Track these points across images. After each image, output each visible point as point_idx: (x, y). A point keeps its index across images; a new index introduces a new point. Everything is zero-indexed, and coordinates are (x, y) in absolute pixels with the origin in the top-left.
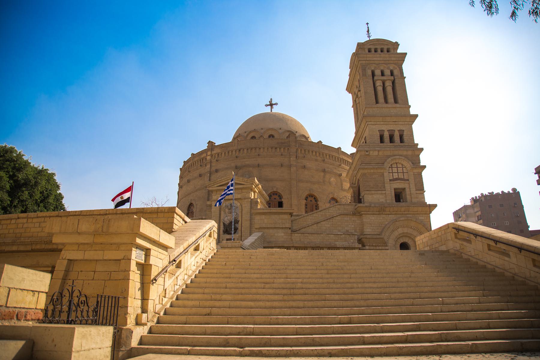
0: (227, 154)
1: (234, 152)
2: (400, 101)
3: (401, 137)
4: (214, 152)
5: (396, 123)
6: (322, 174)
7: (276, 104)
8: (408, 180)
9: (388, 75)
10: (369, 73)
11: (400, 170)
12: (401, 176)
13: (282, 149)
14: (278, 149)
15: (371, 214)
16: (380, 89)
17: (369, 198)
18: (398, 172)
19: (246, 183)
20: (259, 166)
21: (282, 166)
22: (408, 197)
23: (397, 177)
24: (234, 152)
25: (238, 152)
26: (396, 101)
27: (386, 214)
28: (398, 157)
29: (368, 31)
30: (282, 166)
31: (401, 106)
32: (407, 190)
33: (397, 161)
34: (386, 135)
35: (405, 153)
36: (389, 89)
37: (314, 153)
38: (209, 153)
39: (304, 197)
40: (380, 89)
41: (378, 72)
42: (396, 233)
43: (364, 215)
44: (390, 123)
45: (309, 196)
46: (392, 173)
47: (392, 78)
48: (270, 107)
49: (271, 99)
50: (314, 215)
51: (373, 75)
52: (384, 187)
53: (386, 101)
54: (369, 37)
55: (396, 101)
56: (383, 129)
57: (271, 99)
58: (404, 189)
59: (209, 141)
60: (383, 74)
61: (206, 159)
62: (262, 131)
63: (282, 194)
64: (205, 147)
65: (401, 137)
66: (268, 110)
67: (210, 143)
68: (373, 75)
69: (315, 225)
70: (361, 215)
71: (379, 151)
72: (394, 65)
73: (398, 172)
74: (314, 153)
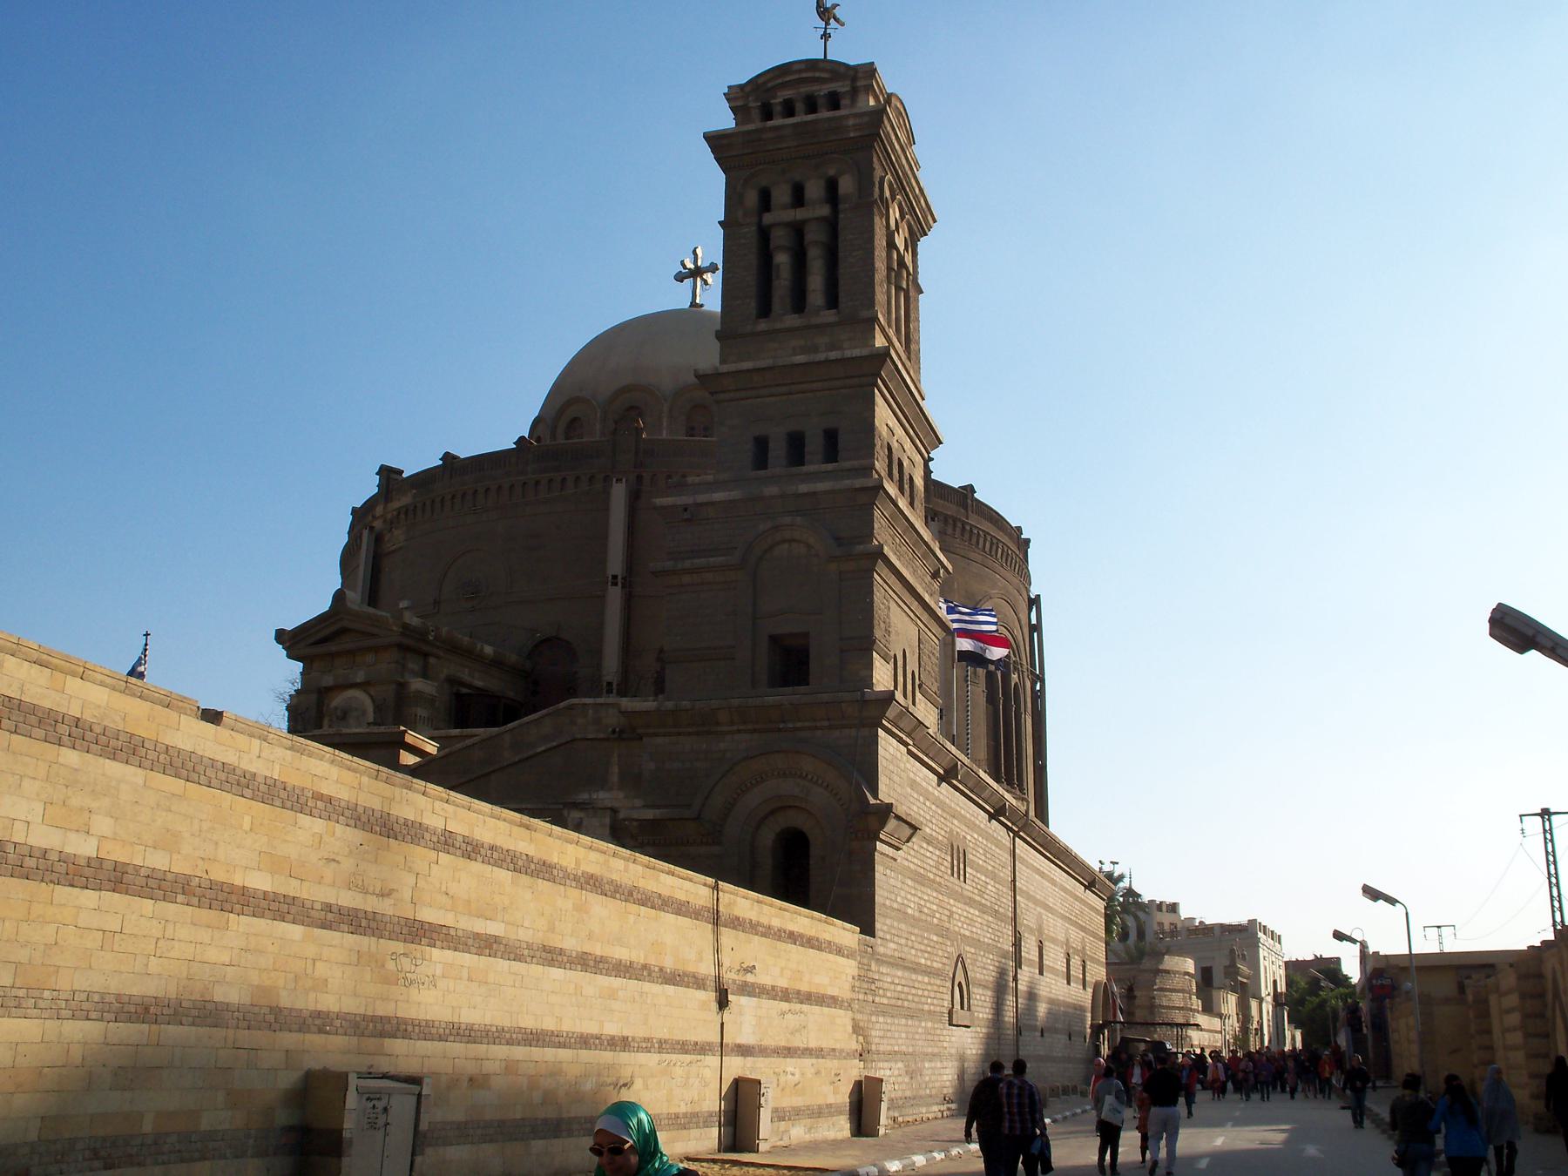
3: (831, 437)
4: (395, 505)
10: (752, 198)
16: (782, 259)
26: (833, 301)
38: (379, 510)
41: (781, 195)
51: (765, 202)
53: (799, 302)
54: (826, 36)
55: (833, 301)
58: (806, 635)
60: (799, 198)
65: (831, 437)
66: (677, 298)
67: (388, 475)
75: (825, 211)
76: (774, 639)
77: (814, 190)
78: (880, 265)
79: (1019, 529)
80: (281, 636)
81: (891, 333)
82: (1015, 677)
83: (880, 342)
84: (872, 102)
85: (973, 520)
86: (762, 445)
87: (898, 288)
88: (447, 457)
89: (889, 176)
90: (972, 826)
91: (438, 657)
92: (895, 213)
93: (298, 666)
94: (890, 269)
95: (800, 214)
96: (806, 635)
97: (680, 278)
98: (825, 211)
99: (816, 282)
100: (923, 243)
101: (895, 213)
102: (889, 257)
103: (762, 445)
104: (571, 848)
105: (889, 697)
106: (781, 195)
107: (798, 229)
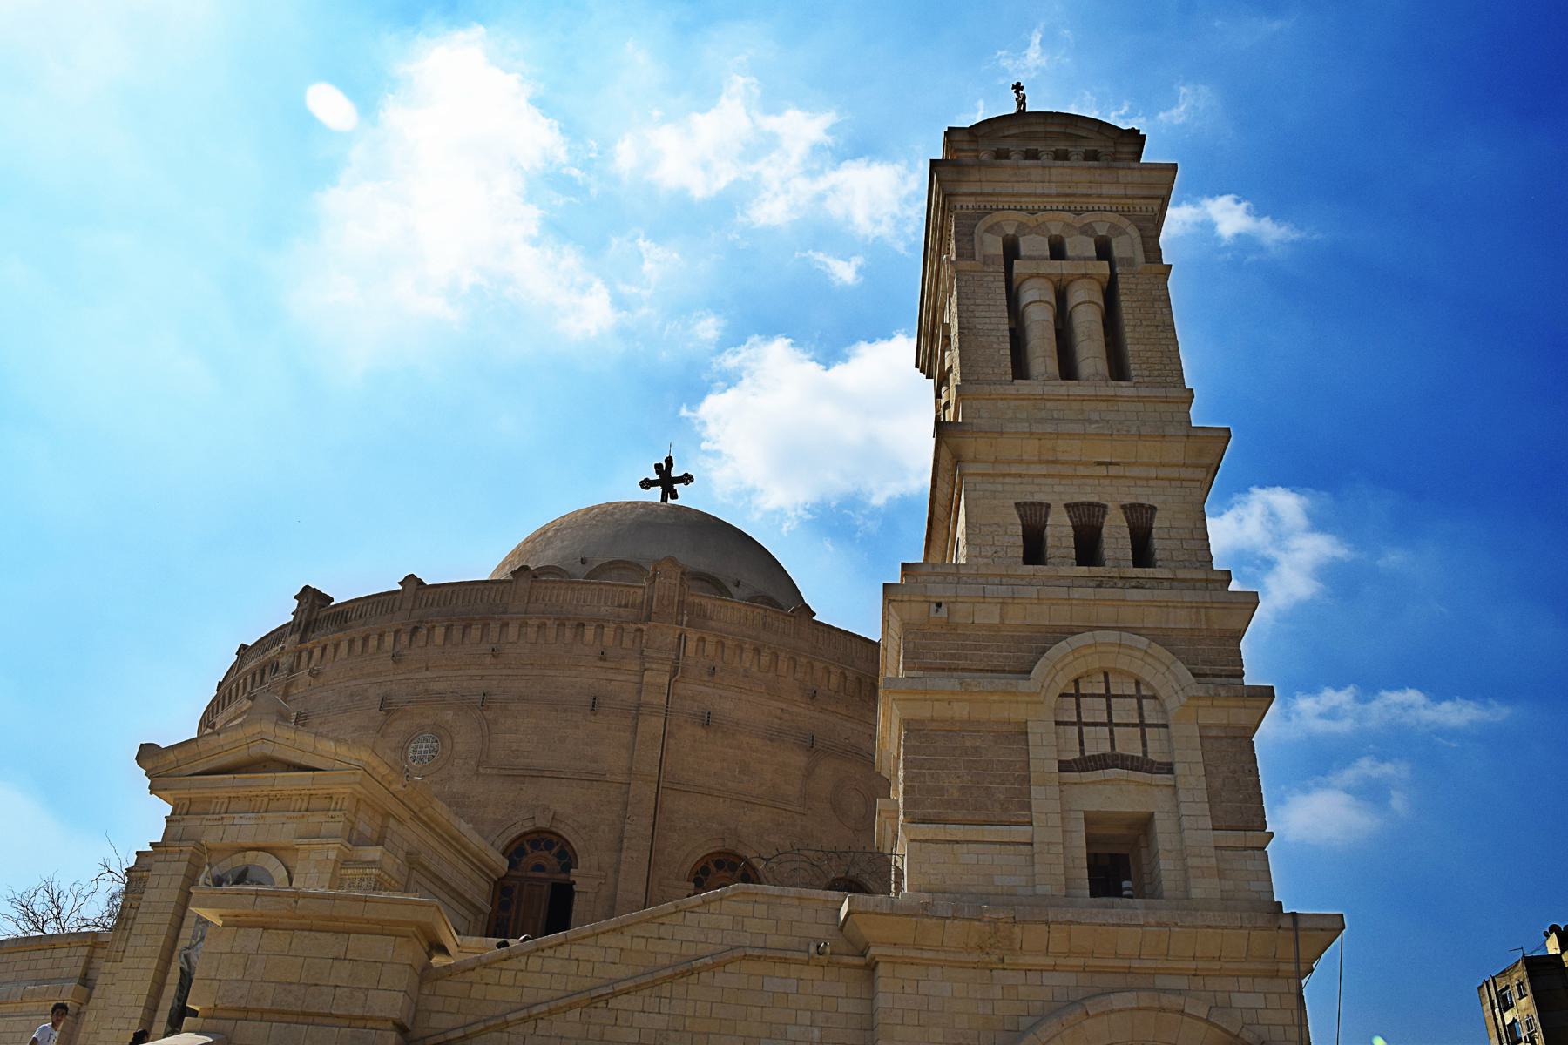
0: (358, 644)
1: (389, 640)
2: (1134, 368)
5: (1113, 470)
6: (799, 759)
7: (687, 479)
10: (995, 247)
11: (1124, 711)
12: (1128, 743)
13: (609, 632)
14: (589, 633)
16: (1039, 319)
18: (1110, 724)
20: (485, 700)
21: (594, 705)
22: (1167, 867)
23: (1105, 748)
24: (389, 640)
25: (404, 638)
28: (1113, 636)
30: (594, 705)
31: (1144, 392)
32: (1162, 825)
34: (1059, 531)
35: (1152, 619)
36: (1087, 321)
37: (765, 659)
39: (687, 868)
40: (1039, 319)
43: (882, 970)
44: (1081, 470)
45: (719, 865)
46: (1080, 724)
47: (1103, 268)
48: (658, 490)
49: (669, 461)
50: (577, 951)
51: (1011, 251)
52: (1029, 808)
56: (1039, 497)
57: (669, 461)
60: (1057, 251)
61: (275, 667)
62: (588, 568)
63: (577, 843)
64: (283, 612)
67: (311, 599)
68: (1011, 251)
69: (574, 1015)
70: (872, 967)
72: (1114, 218)
73: (1110, 724)
74: (765, 659)
80: (147, 754)
91: (401, 822)
99: (1090, 353)
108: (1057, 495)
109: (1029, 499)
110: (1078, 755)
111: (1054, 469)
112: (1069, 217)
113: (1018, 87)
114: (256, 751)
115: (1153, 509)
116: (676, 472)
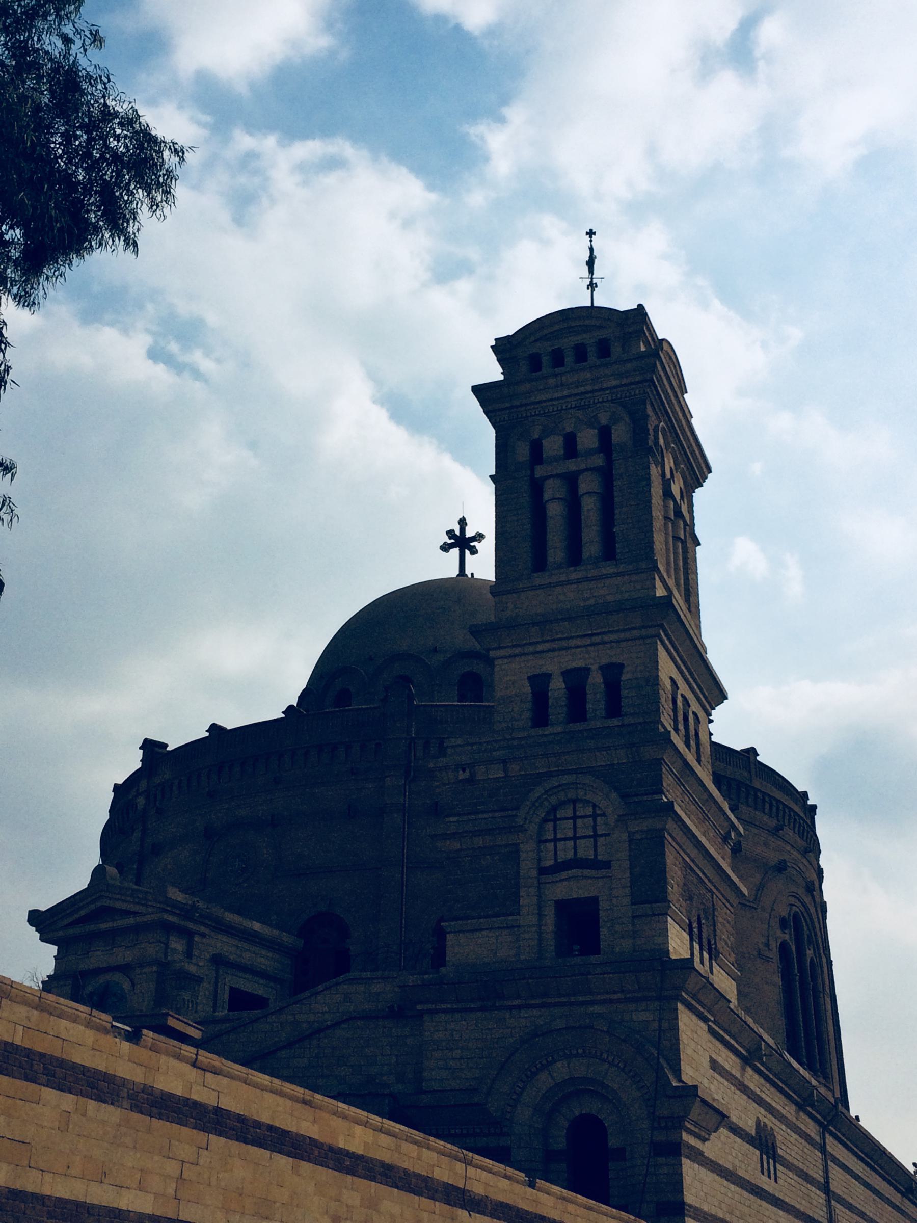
3: (613, 689)
4: (157, 780)
8: (607, 865)
9: (590, 453)
10: (523, 452)
12: (585, 850)
15: (453, 1011)
16: (555, 510)
17: (469, 947)
19: (142, 909)
23: (570, 855)
26: (609, 553)
27: (511, 1008)
29: (591, 263)
32: (603, 905)
33: (571, 794)
36: (590, 506)
38: (143, 785)
40: (555, 510)
41: (553, 445)
42: (544, 1081)
43: (426, 1017)
44: (573, 643)
49: (463, 522)
53: (575, 557)
54: (592, 286)
57: (463, 522)
58: (595, 901)
59: (146, 740)
60: (571, 448)
64: (133, 762)
65: (613, 689)
66: (445, 567)
67: (151, 748)
71: (504, 762)
73: (575, 838)
75: (599, 460)
76: (561, 906)
77: (588, 439)
78: (657, 513)
79: (805, 795)
80: (35, 918)
81: (671, 583)
82: (810, 953)
83: (660, 592)
84: (643, 348)
85: (757, 784)
86: (540, 698)
87: (676, 538)
88: (214, 729)
89: (662, 424)
90: (782, 1118)
91: (203, 935)
92: (669, 463)
93: (53, 949)
94: (666, 518)
95: (572, 466)
96: (595, 901)
97: (445, 548)
98: (599, 460)
100: (699, 495)
101: (669, 463)
102: (666, 506)
103: (540, 698)
104: (358, 1130)
105: (686, 965)
106: (553, 445)
107: (572, 480)
108: (554, 665)
109: (538, 671)
110: (552, 863)
111: (555, 645)
112: (580, 414)
113: (591, 233)
114: (99, 904)
115: (622, 666)
116: (469, 533)
